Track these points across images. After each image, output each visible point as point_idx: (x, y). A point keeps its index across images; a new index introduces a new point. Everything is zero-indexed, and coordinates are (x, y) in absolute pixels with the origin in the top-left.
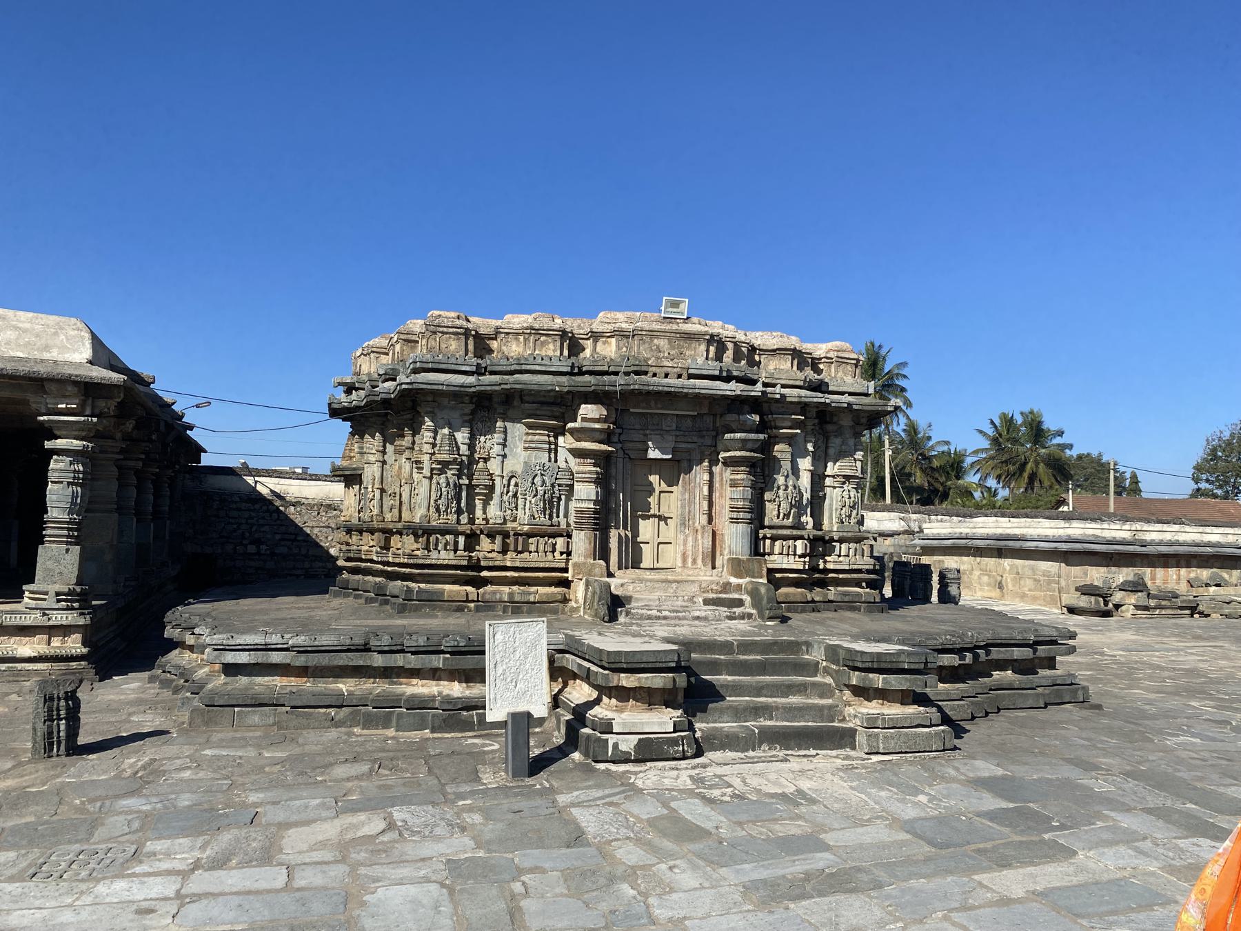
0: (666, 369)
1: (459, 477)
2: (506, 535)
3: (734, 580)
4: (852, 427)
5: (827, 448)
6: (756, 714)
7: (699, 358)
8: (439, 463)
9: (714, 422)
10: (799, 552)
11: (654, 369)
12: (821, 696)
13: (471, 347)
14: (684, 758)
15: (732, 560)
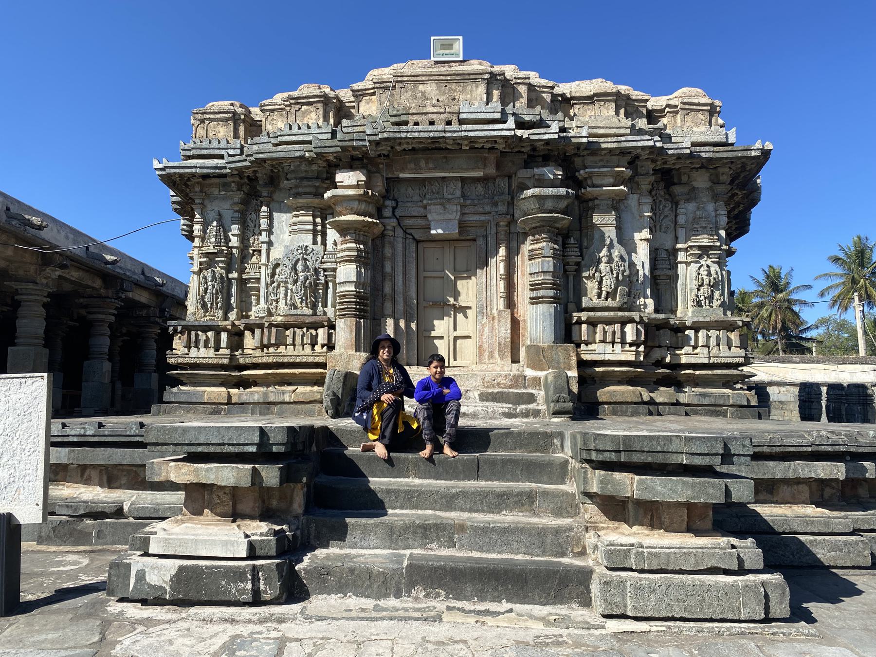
0: (430, 116)
1: (229, 271)
2: (261, 326)
3: (530, 373)
4: (710, 189)
5: (676, 216)
6: (425, 536)
7: (475, 101)
8: (207, 255)
9: (510, 186)
10: (630, 337)
11: (415, 118)
12: (558, 513)
13: (242, 133)
14: (256, 601)
15: (528, 347)
